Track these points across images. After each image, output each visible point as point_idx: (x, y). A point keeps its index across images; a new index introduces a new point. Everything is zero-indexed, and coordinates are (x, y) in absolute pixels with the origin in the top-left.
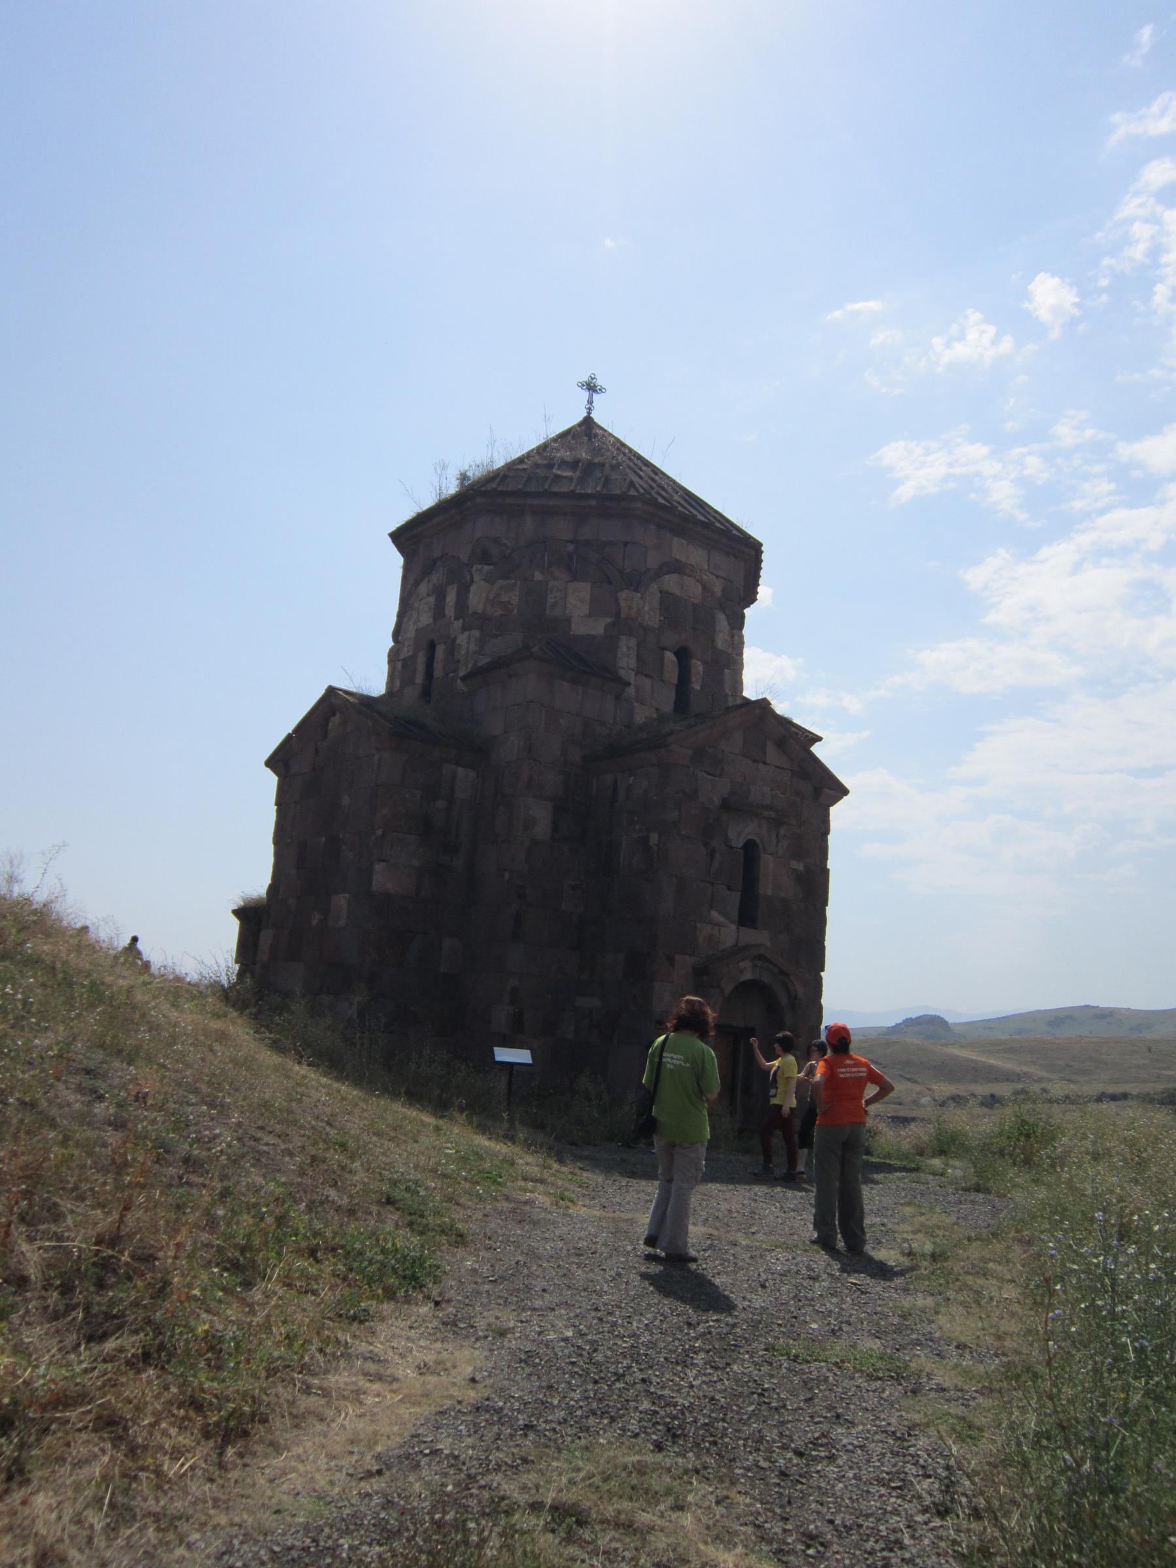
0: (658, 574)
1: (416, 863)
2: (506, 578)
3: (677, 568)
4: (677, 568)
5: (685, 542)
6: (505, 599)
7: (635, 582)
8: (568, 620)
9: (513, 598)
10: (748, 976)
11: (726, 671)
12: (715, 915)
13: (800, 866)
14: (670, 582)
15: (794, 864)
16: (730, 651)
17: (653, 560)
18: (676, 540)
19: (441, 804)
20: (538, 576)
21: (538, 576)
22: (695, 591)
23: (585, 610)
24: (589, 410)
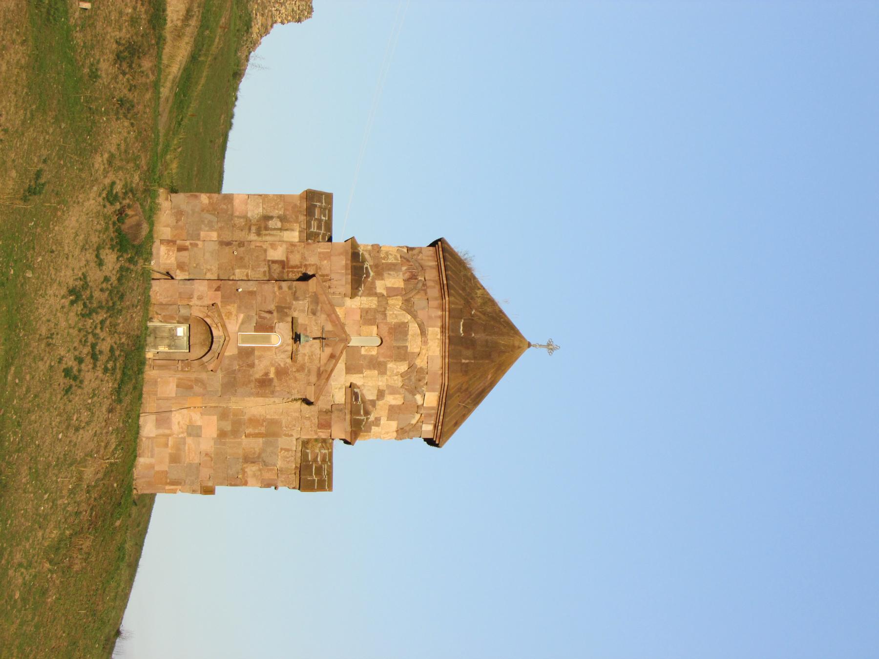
0: (415, 317)
1: (249, 215)
2: (401, 257)
3: (423, 333)
4: (423, 333)
5: (439, 336)
6: (390, 257)
7: (409, 307)
8: (382, 279)
9: (391, 260)
10: (215, 333)
11: (376, 372)
12: (242, 316)
13: (272, 375)
14: (414, 328)
15: (272, 371)
16: (388, 373)
17: (421, 315)
18: (438, 330)
19: (279, 225)
20: (404, 268)
21: (404, 268)
22: (414, 344)
23: (389, 285)
24: (535, 346)
